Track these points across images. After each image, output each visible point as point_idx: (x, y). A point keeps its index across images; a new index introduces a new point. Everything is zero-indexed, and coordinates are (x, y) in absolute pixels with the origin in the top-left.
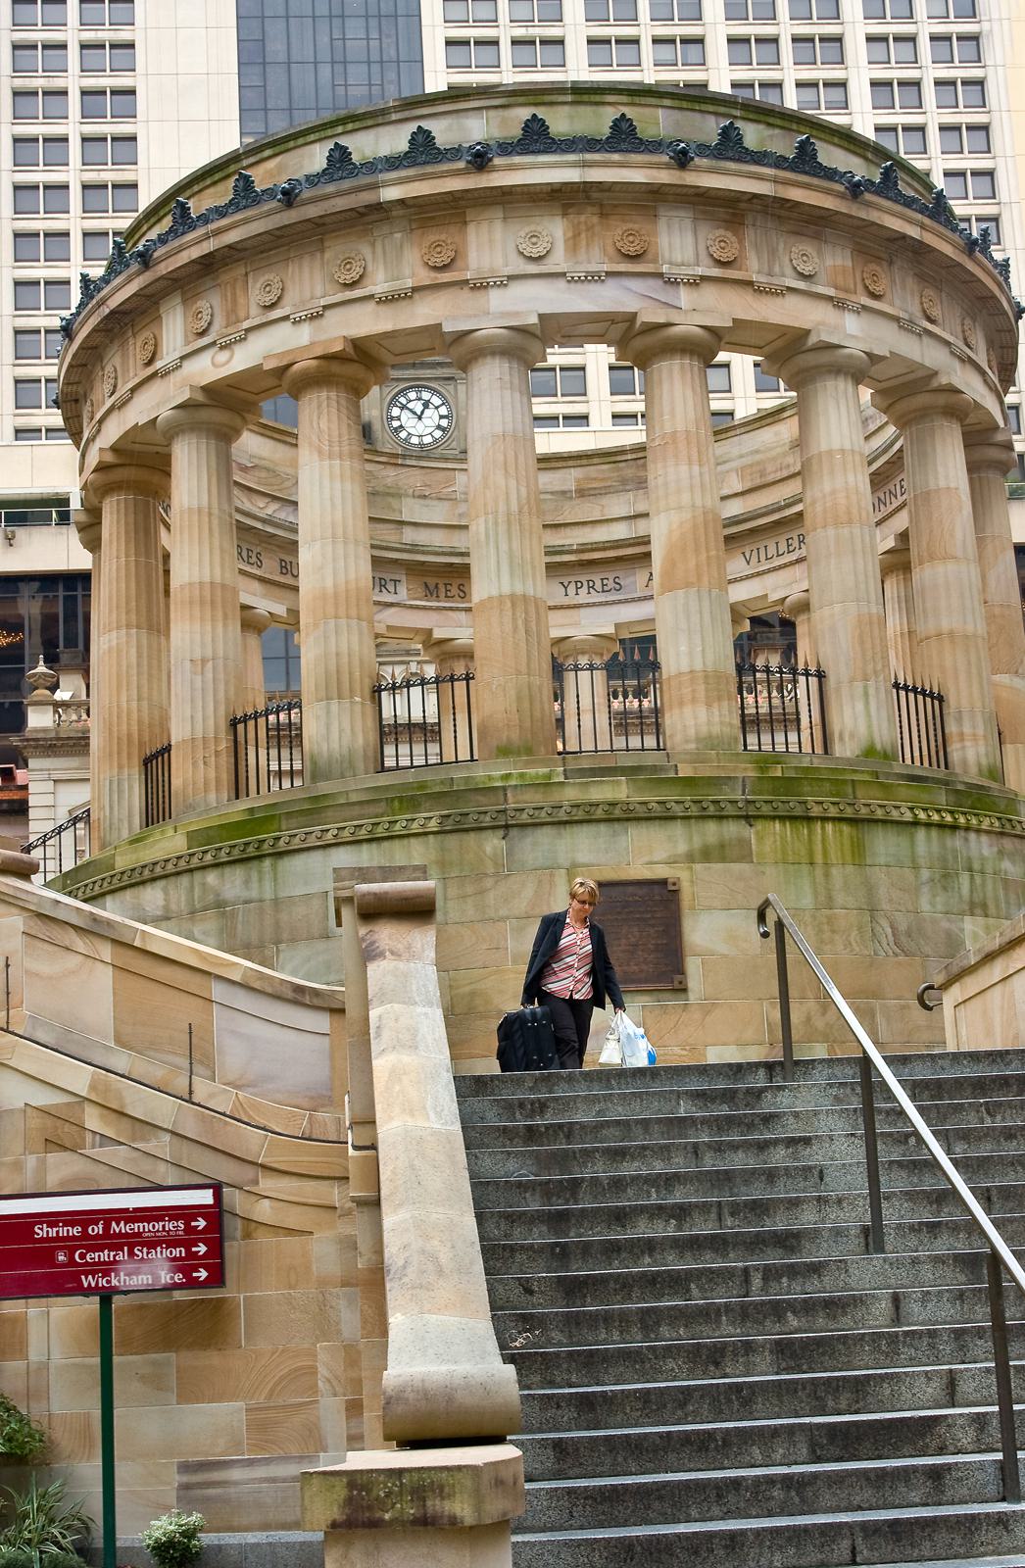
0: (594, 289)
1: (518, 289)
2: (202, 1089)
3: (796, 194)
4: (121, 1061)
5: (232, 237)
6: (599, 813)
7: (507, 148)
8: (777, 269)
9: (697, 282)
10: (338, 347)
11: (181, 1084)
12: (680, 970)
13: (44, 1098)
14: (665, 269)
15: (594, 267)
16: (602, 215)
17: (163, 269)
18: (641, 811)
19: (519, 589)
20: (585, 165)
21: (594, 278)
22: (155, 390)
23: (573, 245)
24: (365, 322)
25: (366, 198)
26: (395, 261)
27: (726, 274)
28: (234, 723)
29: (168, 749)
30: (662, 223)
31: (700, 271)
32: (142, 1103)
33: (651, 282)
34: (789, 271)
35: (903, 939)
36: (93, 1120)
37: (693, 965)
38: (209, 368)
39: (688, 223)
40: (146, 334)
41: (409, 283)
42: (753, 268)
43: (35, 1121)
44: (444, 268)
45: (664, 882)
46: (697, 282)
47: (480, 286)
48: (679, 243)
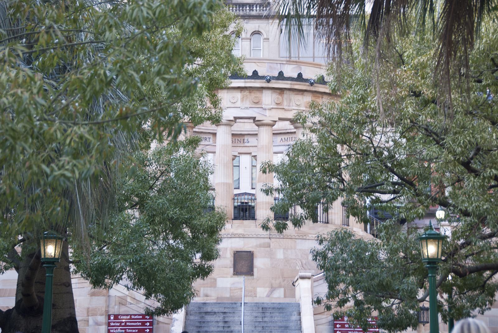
0: (246, 111)
1: (229, 110)
6: (237, 236)
8: (291, 104)
9: (270, 109)
12: (252, 271)
14: (263, 106)
15: (247, 106)
16: (250, 92)
19: (225, 182)
20: (245, 82)
21: (247, 108)
27: (279, 106)
30: (264, 94)
31: (272, 107)
33: (260, 109)
34: (294, 104)
35: (304, 266)
36: (129, 300)
37: (255, 270)
39: (270, 94)
42: (285, 105)
43: (117, 299)
45: (250, 252)
46: (270, 109)
48: (268, 98)
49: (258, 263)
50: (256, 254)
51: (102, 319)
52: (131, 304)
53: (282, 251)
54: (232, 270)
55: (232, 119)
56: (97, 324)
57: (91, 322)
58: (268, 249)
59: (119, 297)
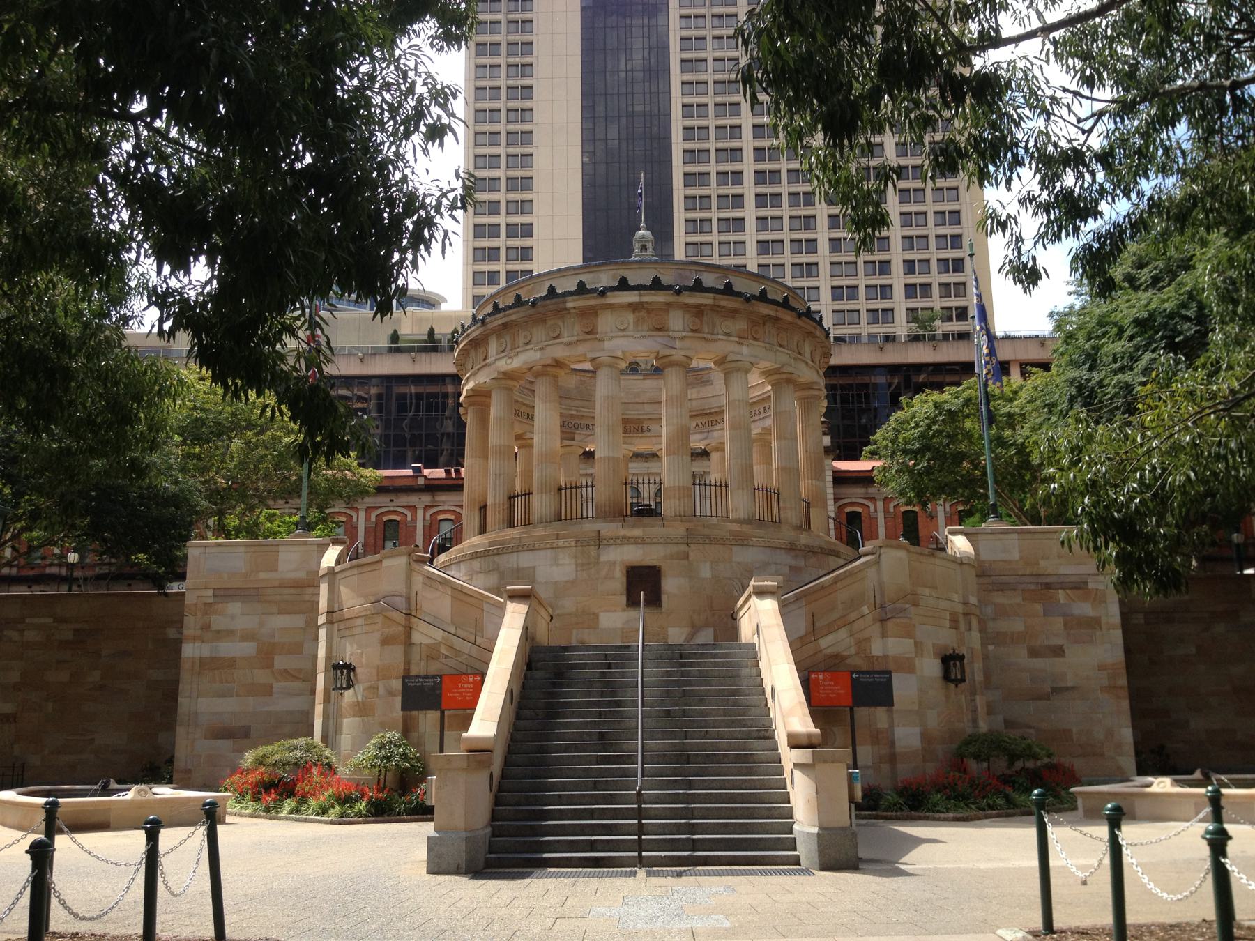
2: (479, 641)
3: (723, 303)
4: (453, 630)
5: (513, 317)
7: (612, 289)
9: (682, 338)
10: (549, 362)
11: (472, 638)
13: (427, 641)
17: (489, 326)
18: (648, 541)
22: (486, 370)
23: (637, 323)
24: (559, 352)
25: (562, 306)
26: (571, 330)
28: (510, 498)
29: (486, 506)
32: (458, 644)
36: (443, 650)
37: (664, 598)
38: (505, 365)
40: (482, 350)
41: (575, 338)
44: (588, 333)
45: (654, 567)
46: (682, 338)
47: (602, 340)
49: (670, 585)
50: (664, 569)
51: (397, 685)
52: (446, 657)
53: (708, 564)
54: (624, 599)
55: (619, 354)
56: (391, 693)
57: (381, 691)
58: (685, 562)
59: (428, 646)
